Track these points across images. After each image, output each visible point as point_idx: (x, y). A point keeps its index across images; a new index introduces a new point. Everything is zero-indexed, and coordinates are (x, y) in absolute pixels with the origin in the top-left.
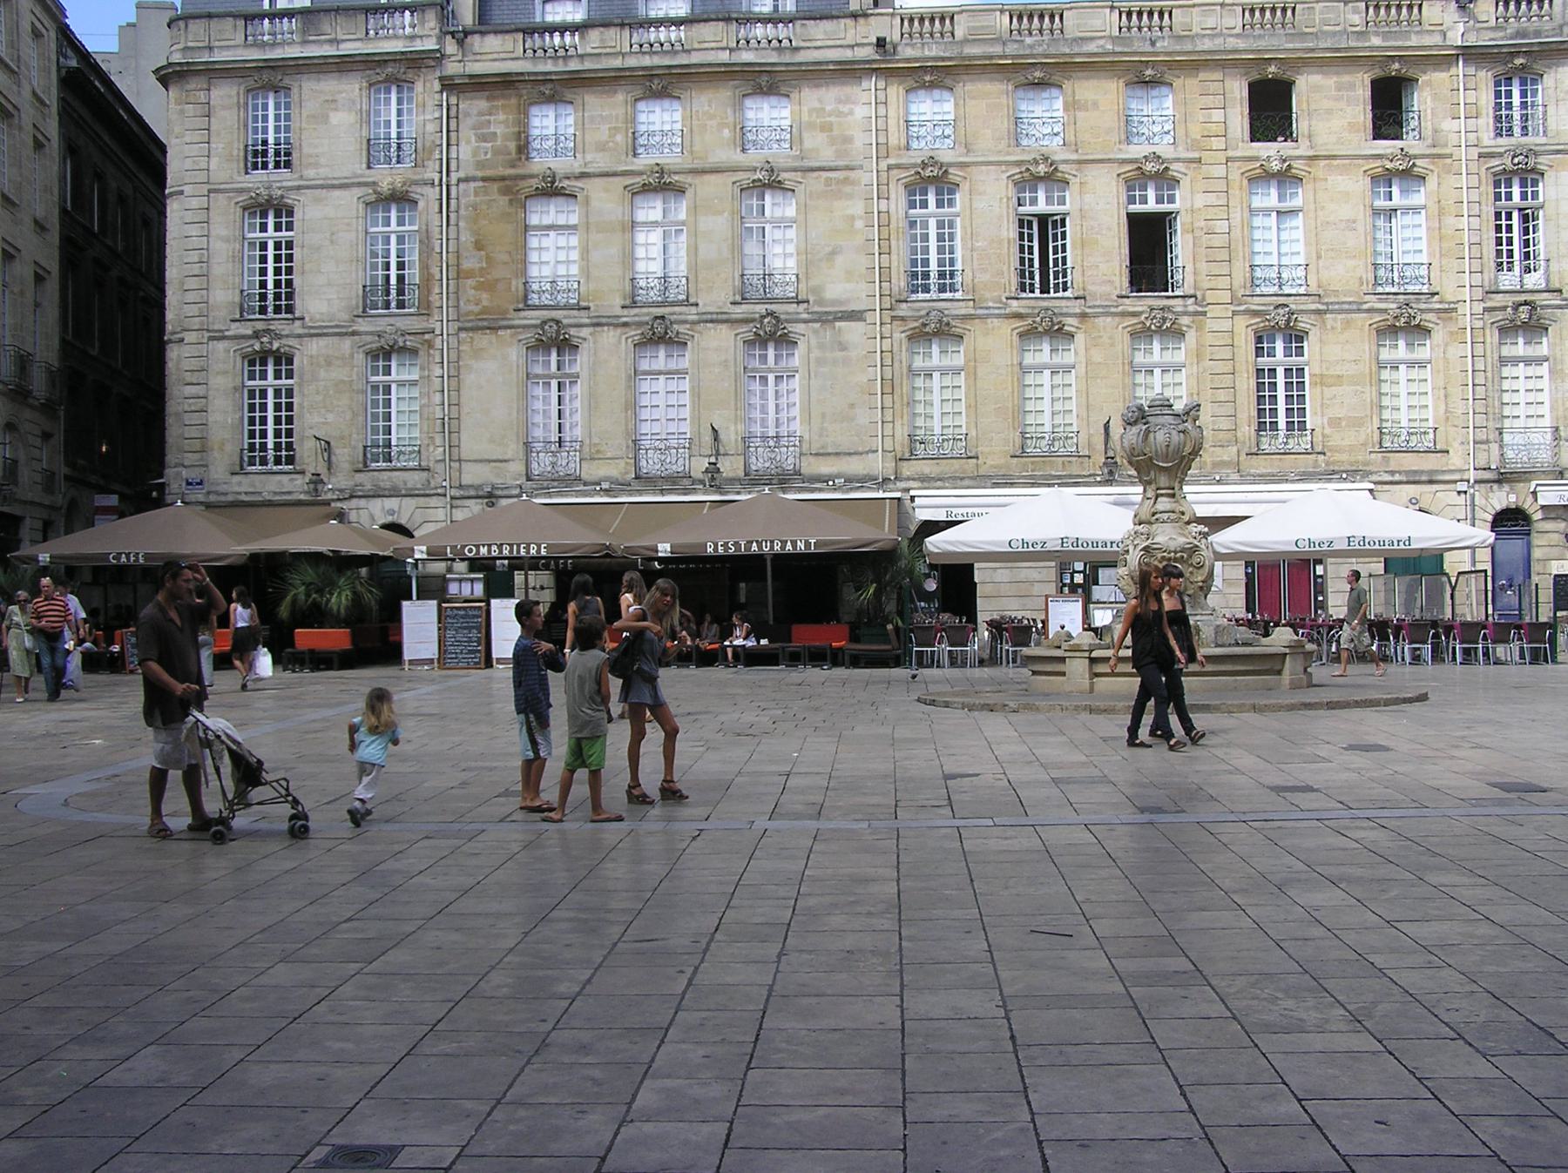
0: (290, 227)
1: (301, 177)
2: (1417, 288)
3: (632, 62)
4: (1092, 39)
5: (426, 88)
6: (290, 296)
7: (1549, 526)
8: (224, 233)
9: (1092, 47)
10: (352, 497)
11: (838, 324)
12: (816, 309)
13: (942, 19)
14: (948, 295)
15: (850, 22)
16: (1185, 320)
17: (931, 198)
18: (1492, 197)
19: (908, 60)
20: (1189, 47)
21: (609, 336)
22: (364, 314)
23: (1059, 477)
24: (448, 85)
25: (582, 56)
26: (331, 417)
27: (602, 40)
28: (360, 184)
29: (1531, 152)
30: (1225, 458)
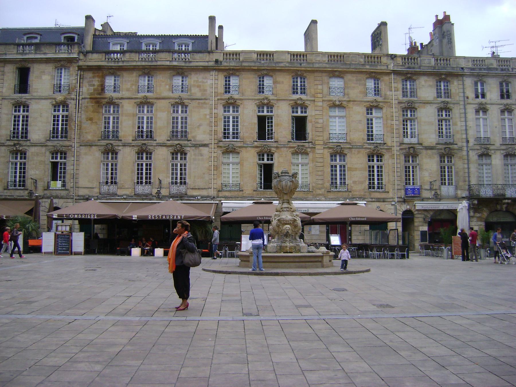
0: (28, 111)
1: (32, 96)
2: (380, 142)
3: (139, 64)
4: (282, 62)
5: (73, 69)
6: (26, 133)
7: (419, 216)
8: (6, 112)
9: (282, 65)
10: (43, 198)
11: (200, 148)
12: (194, 143)
13: (236, 55)
14: (235, 140)
15: (207, 54)
16: (309, 150)
17: (231, 109)
18: (402, 115)
19: (225, 66)
20: (312, 66)
21: (128, 150)
22: (49, 140)
23: (269, 198)
24: (80, 68)
25: (123, 62)
26: (37, 172)
27: (130, 57)
28: (50, 99)
29: (412, 102)
30: (321, 193)
